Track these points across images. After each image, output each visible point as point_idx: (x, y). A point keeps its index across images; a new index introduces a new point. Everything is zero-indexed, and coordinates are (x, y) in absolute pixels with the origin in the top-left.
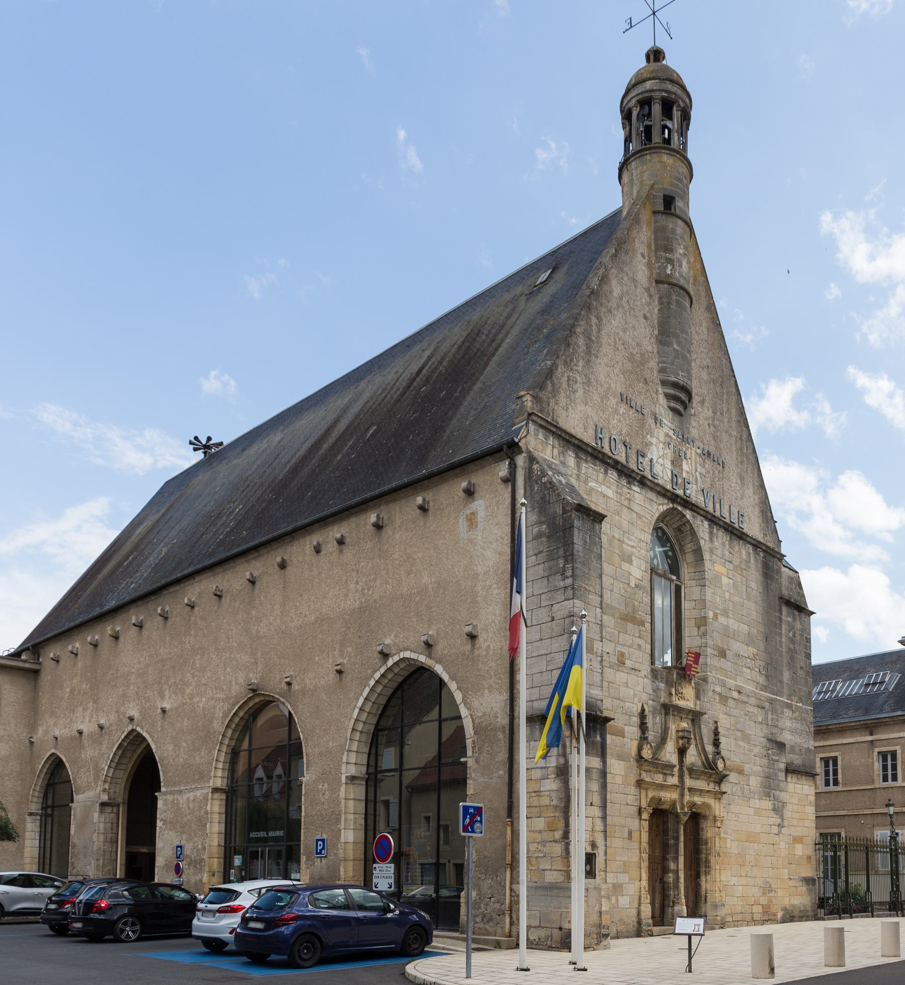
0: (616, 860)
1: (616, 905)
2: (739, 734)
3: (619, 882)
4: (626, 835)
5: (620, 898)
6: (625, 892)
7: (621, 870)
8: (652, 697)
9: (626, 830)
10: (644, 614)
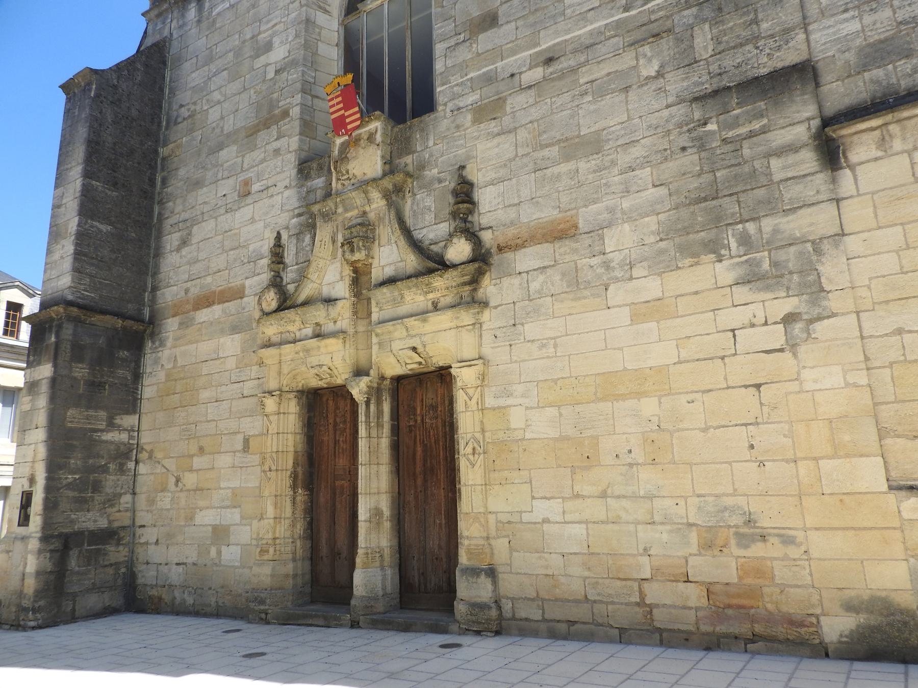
0: (221, 488)
1: (217, 561)
2: (554, 151)
3: (223, 523)
4: (239, 446)
5: (224, 549)
6: (232, 539)
7: (228, 503)
8: (296, 212)
9: (240, 437)
10: (288, 100)
